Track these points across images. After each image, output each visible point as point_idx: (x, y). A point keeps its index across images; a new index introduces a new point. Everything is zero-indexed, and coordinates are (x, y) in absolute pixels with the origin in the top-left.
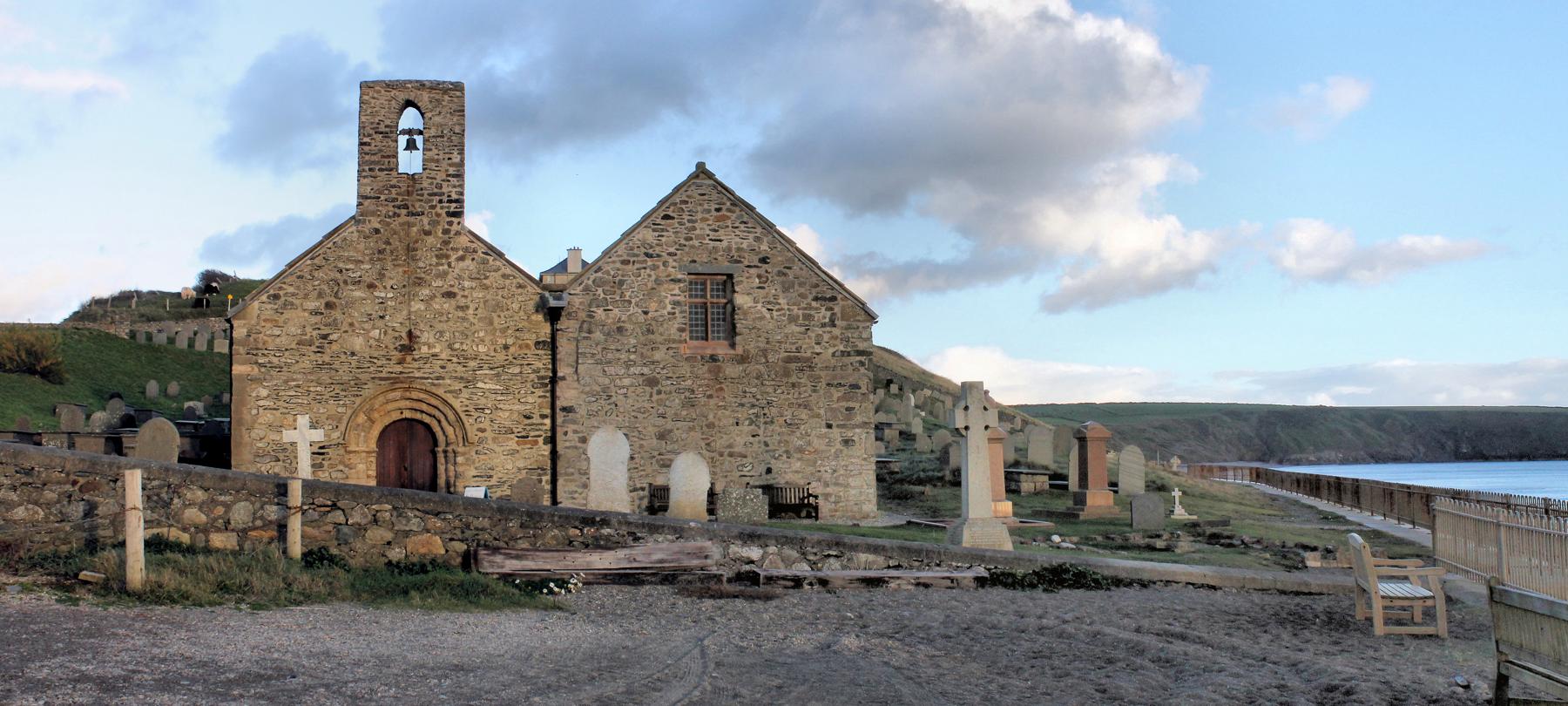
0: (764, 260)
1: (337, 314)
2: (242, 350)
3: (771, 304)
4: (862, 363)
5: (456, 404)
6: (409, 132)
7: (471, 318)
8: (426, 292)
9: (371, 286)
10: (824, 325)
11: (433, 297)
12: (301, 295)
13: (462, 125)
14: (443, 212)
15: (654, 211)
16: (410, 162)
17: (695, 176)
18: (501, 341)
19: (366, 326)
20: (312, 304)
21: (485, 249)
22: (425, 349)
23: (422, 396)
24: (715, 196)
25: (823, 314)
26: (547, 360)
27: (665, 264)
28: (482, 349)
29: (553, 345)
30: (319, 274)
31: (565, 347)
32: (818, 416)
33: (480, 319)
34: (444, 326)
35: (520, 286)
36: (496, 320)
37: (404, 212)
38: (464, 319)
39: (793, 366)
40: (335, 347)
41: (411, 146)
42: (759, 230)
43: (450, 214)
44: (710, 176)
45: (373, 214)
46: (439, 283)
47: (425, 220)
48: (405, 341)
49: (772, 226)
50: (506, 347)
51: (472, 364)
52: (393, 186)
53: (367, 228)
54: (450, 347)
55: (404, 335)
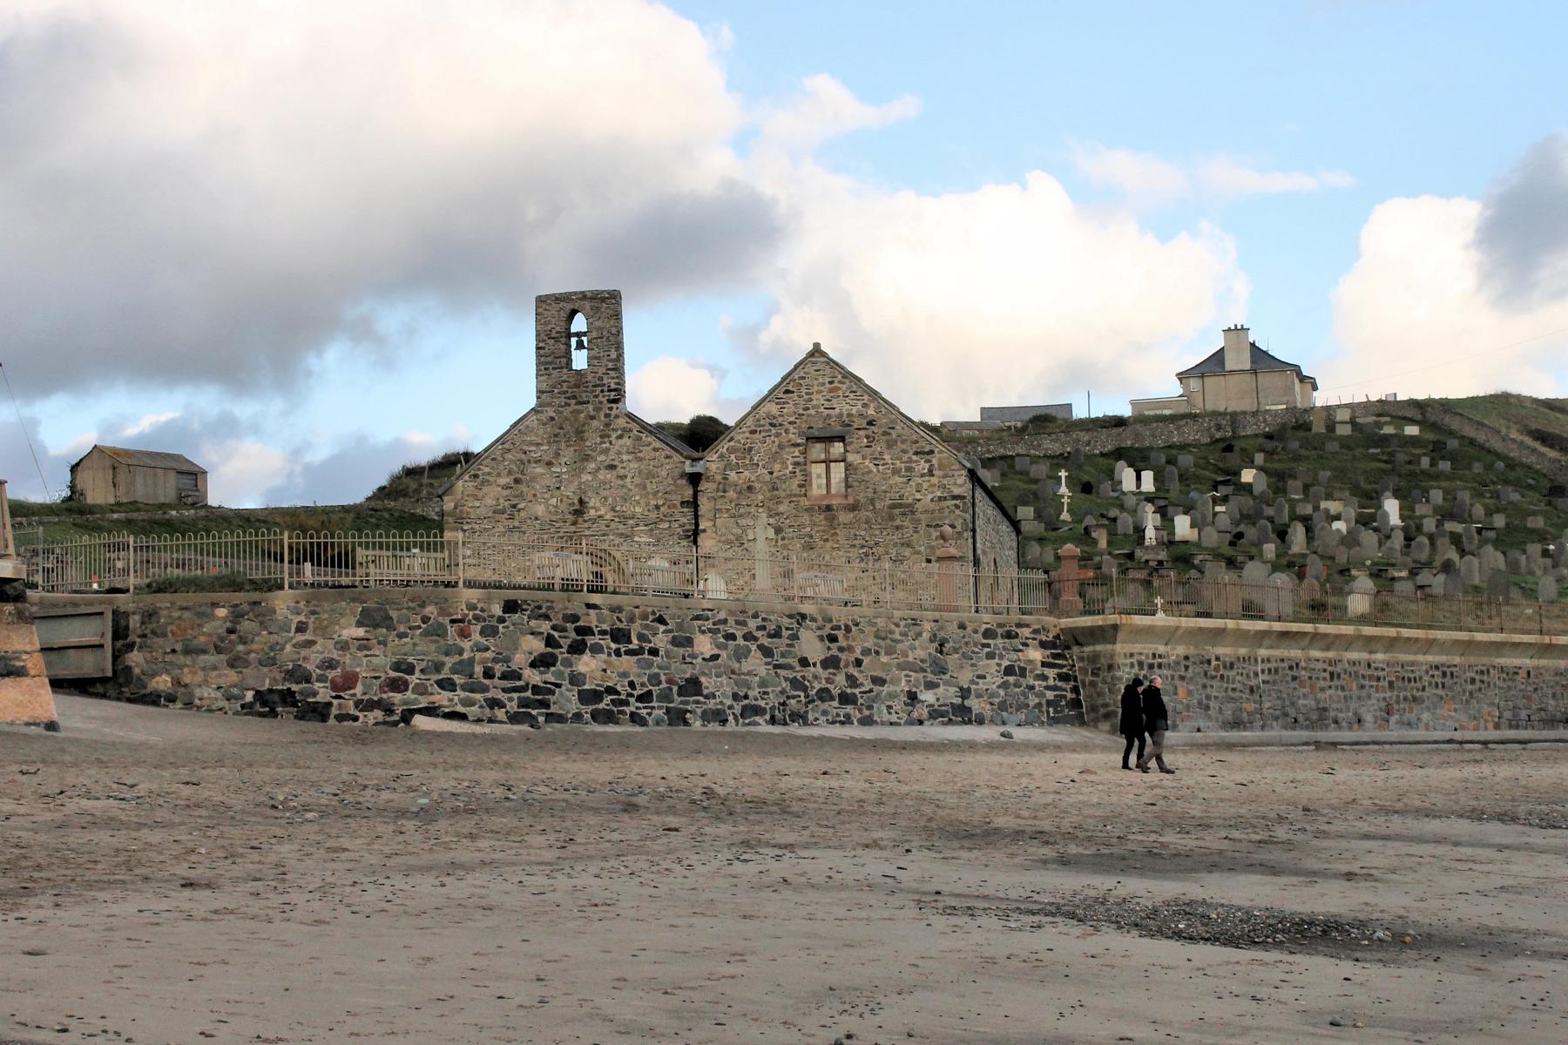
0: (871, 423)
1: (523, 488)
2: (450, 520)
3: (876, 460)
4: (957, 507)
5: (618, 555)
6: (578, 335)
8: (592, 466)
9: (549, 464)
10: (923, 475)
15: (776, 387)
16: (580, 360)
17: (811, 354)
18: (653, 502)
20: (503, 481)
22: (592, 512)
24: (828, 371)
25: (923, 466)
26: (690, 516)
27: (786, 431)
28: (638, 509)
29: (694, 504)
30: (508, 456)
31: (705, 505)
32: (919, 553)
35: (667, 457)
39: (897, 511)
40: (523, 514)
41: (580, 346)
42: (866, 397)
43: (610, 401)
44: (824, 354)
45: (549, 405)
46: (602, 458)
47: (591, 407)
49: (876, 393)
50: (657, 507)
51: (631, 522)
53: (544, 417)
54: (613, 509)
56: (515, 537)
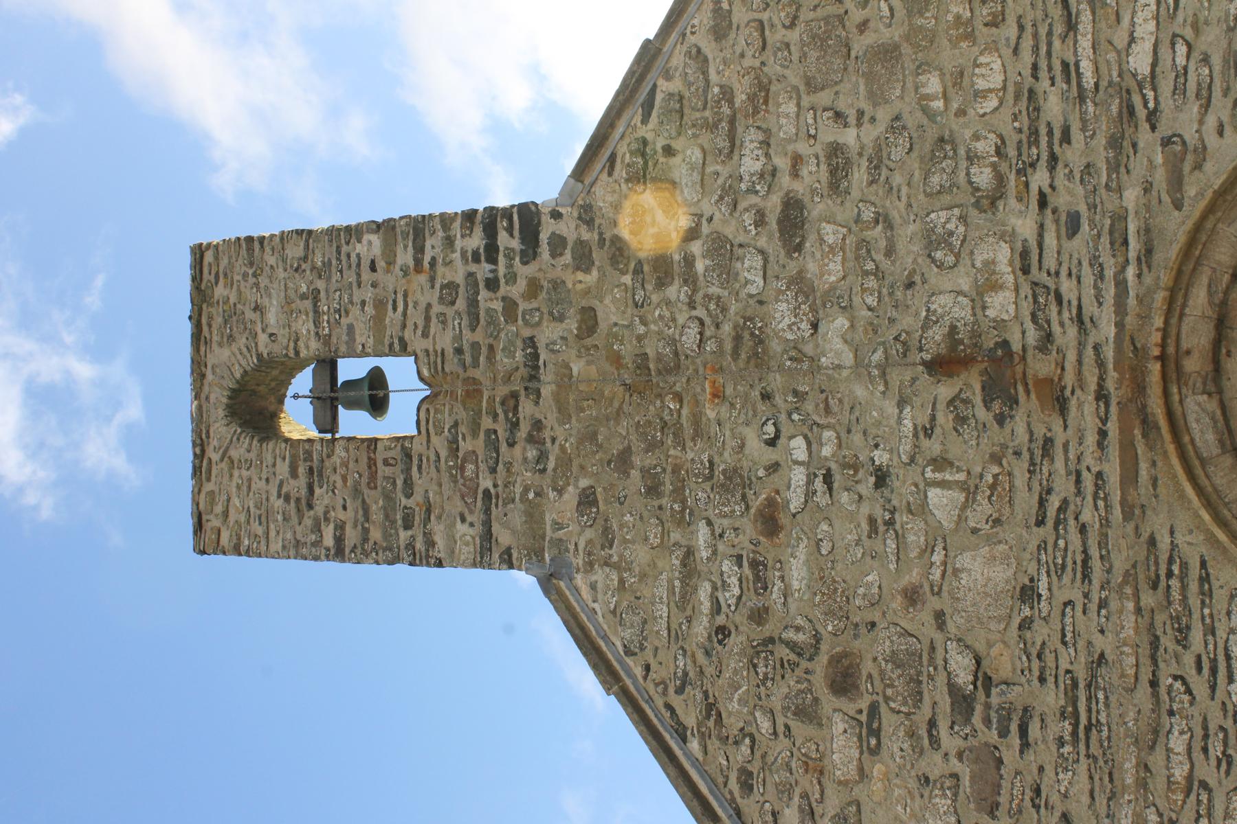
1: (874, 651)
7: (870, 133)
8: (783, 317)
9: (770, 521)
11: (801, 285)
12: (807, 783)
13: (284, 237)
14: (525, 272)
19: (915, 539)
21: (634, 114)
22: (1001, 304)
23: (1199, 299)
28: (992, 73)
30: (732, 707)
33: (877, 98)
34: (908, 231)
36: (882, 34)
37: (526, 408)
38: (877, 163)
40: (1004, 661)
45: (533, 515)
46: (750, 269)
48: (972, 382)
51: (1054, 107)
52: (454, 449)
53: (580, 536)
54: (991, 200)
55: (945, 391)
56: (1126, 712)
